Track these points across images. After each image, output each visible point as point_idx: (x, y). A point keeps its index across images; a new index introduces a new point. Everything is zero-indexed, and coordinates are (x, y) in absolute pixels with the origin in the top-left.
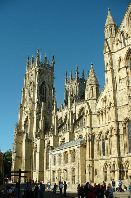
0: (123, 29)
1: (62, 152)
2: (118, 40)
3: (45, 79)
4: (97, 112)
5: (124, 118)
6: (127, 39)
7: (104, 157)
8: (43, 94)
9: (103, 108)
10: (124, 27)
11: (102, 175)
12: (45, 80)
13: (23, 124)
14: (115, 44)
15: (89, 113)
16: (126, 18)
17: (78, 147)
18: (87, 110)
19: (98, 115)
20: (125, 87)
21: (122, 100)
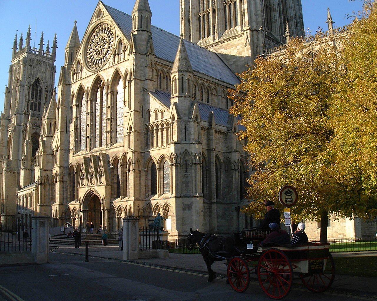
3: (39, 74)
8: (36, 99)
12: (39, 75)
17: (34, 190)
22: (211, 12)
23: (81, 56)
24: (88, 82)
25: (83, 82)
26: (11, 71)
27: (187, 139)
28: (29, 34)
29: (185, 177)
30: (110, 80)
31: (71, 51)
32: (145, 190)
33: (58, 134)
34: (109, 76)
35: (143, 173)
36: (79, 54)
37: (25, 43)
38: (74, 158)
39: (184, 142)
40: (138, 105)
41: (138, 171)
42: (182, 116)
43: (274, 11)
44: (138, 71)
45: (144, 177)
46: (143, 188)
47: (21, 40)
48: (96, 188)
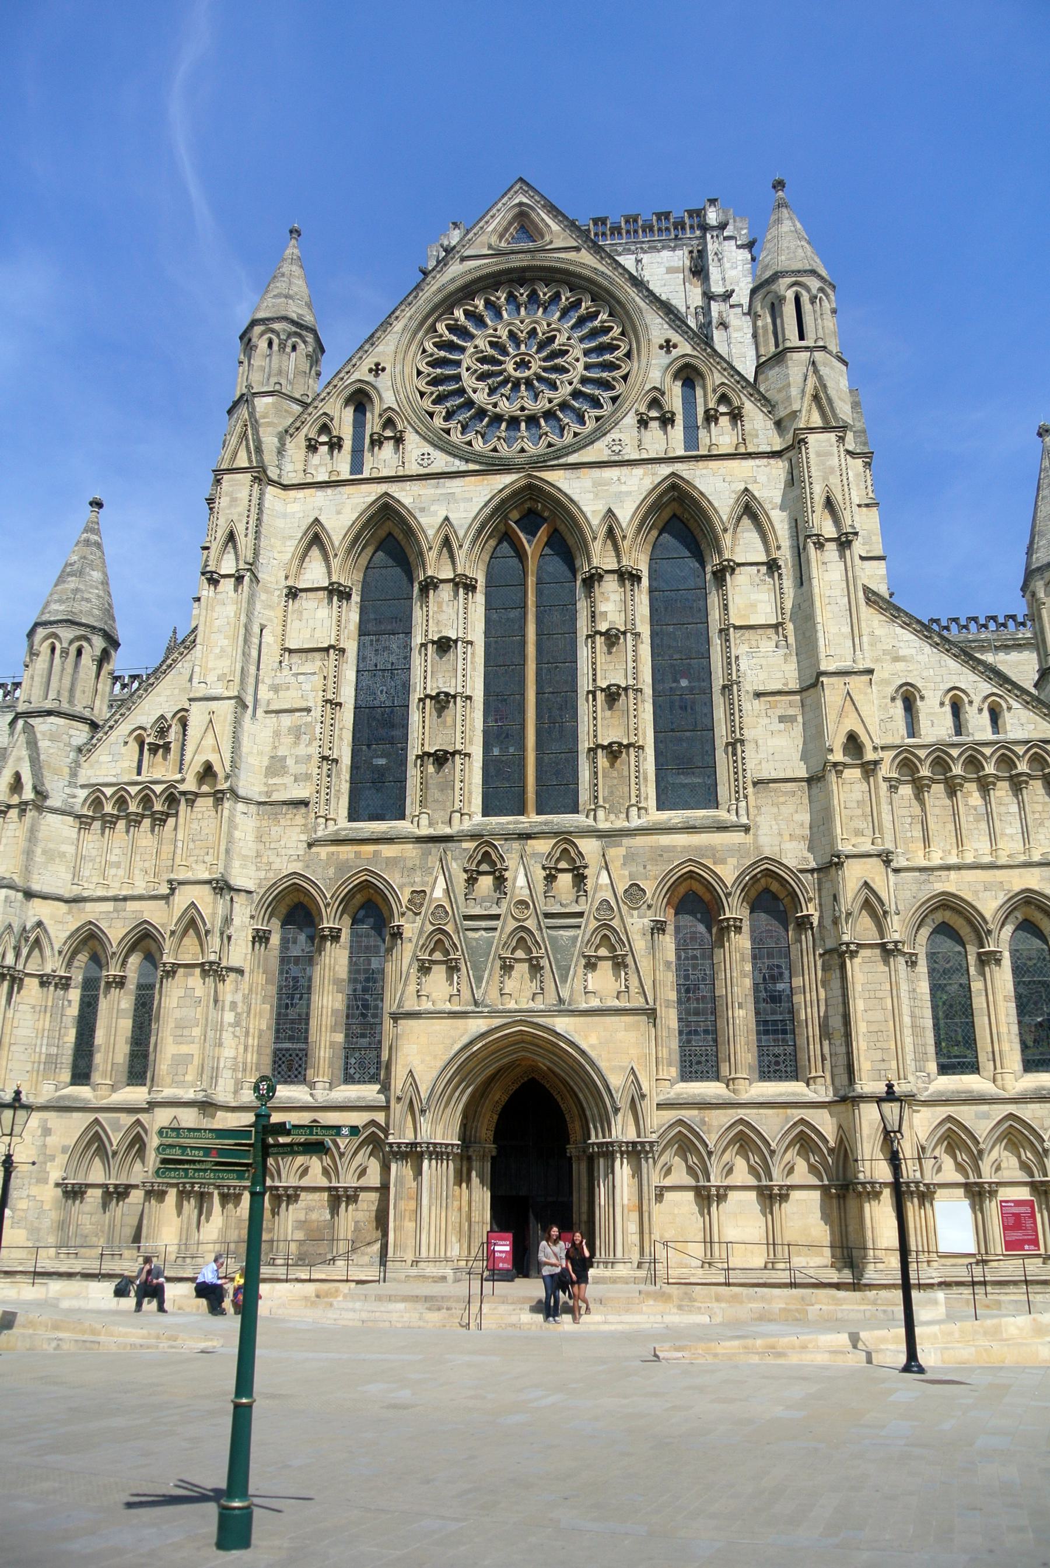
0: (370, 378)
2: (325, 429)
4: (80, 800)
5: (273, 878)
6: (377, 442)
7: (84, 1092)
9: (133, 790)
10: (377, 369)
11: (46, 1207)
14: (300, 439)
15: (28, 794)
16: (398, 326)
18: (18, 777)
19: (83, 822)
20: (315, 701)
21: (276, 766)
24: (450, 498)
25: (406, 495)
30: (626, 514)
34: (620, 496)
36: (369, 362)
38: (314, 849)
48: (562, 1024)
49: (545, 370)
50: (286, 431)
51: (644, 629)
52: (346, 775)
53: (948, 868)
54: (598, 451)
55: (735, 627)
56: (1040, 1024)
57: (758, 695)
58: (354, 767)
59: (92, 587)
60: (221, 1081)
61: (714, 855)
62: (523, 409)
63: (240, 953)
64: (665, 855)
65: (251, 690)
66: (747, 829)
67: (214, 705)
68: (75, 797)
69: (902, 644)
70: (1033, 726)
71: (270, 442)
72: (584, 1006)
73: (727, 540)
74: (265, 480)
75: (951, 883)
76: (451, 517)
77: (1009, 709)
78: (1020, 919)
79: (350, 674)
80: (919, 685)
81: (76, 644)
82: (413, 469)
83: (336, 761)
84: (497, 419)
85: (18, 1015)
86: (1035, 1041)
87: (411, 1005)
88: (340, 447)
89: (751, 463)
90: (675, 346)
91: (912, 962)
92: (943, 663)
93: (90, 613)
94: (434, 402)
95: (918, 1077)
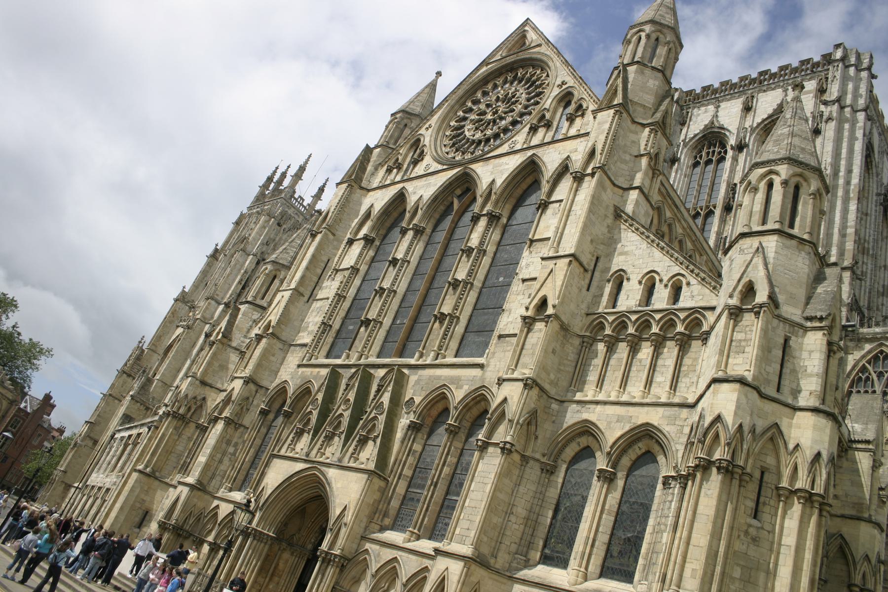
1: (126, 434)
2: (397, 159)
6: (415, 163)
13: (161, 351)
14: (385, 168)
15: (221, 335)
22: (718, 212)
23: (430, 130)
24: (429, 185)
25: (410, 187)
26: (237, 223)
27: (786, 389)
28: (302, 169)
29: (746, 533)
30: (499, 182)
31: (405, 121)
32: (519, 535)
33: (283, 297)
35: (533, 472)
36: (427, 125)
37: (286, 183)
39: (771, 391)
40: (588, 247)
41: (516, 457)
42: (781, 298)
43: (863, 254)
44: (615, 158)
45: (533, 488)
46: (517, 527)
47: (284, 175)
48: (332, 473)
49: (505, 113)
50: (380, 164)
51: (491, 249)
52: (333, 333)
53: (597, 403)
54: (505, 149)
55: (532, 241)
56: (629, 539)
57: (524, 281)
58: (339, 332)
59: (294, 247)
60: (214, 481)
61: (458, 383)
62: (485, 135)
63: (251, 418)
64: (435, 381)
65: (310, 289)
66: (481, 366)
67: (284, 293)
68: (243, 342)
69: (628, 244)
70: (701, 297)
71: (370, 168)
72: (345, 463)
73: (545, 187)
74: (356, 186)
75: (593, 414)
76: (425, 194)
77: (688, 284)
78: (643, 451)
79: (357, 282)
80: (629, 271)
81: (274, 273)
82: (422, 173)
83: (331, 326)
84: (473, 141)
85: (180, 439)
86: (620, 551)
87: (282, 452)
88: (400, 168)
89: (579, 140)
90: (566, 83)
91: (547, 471)
92: (651, 255)
93: (286, 259)
94: (451, 140)
95: (515, 559)
